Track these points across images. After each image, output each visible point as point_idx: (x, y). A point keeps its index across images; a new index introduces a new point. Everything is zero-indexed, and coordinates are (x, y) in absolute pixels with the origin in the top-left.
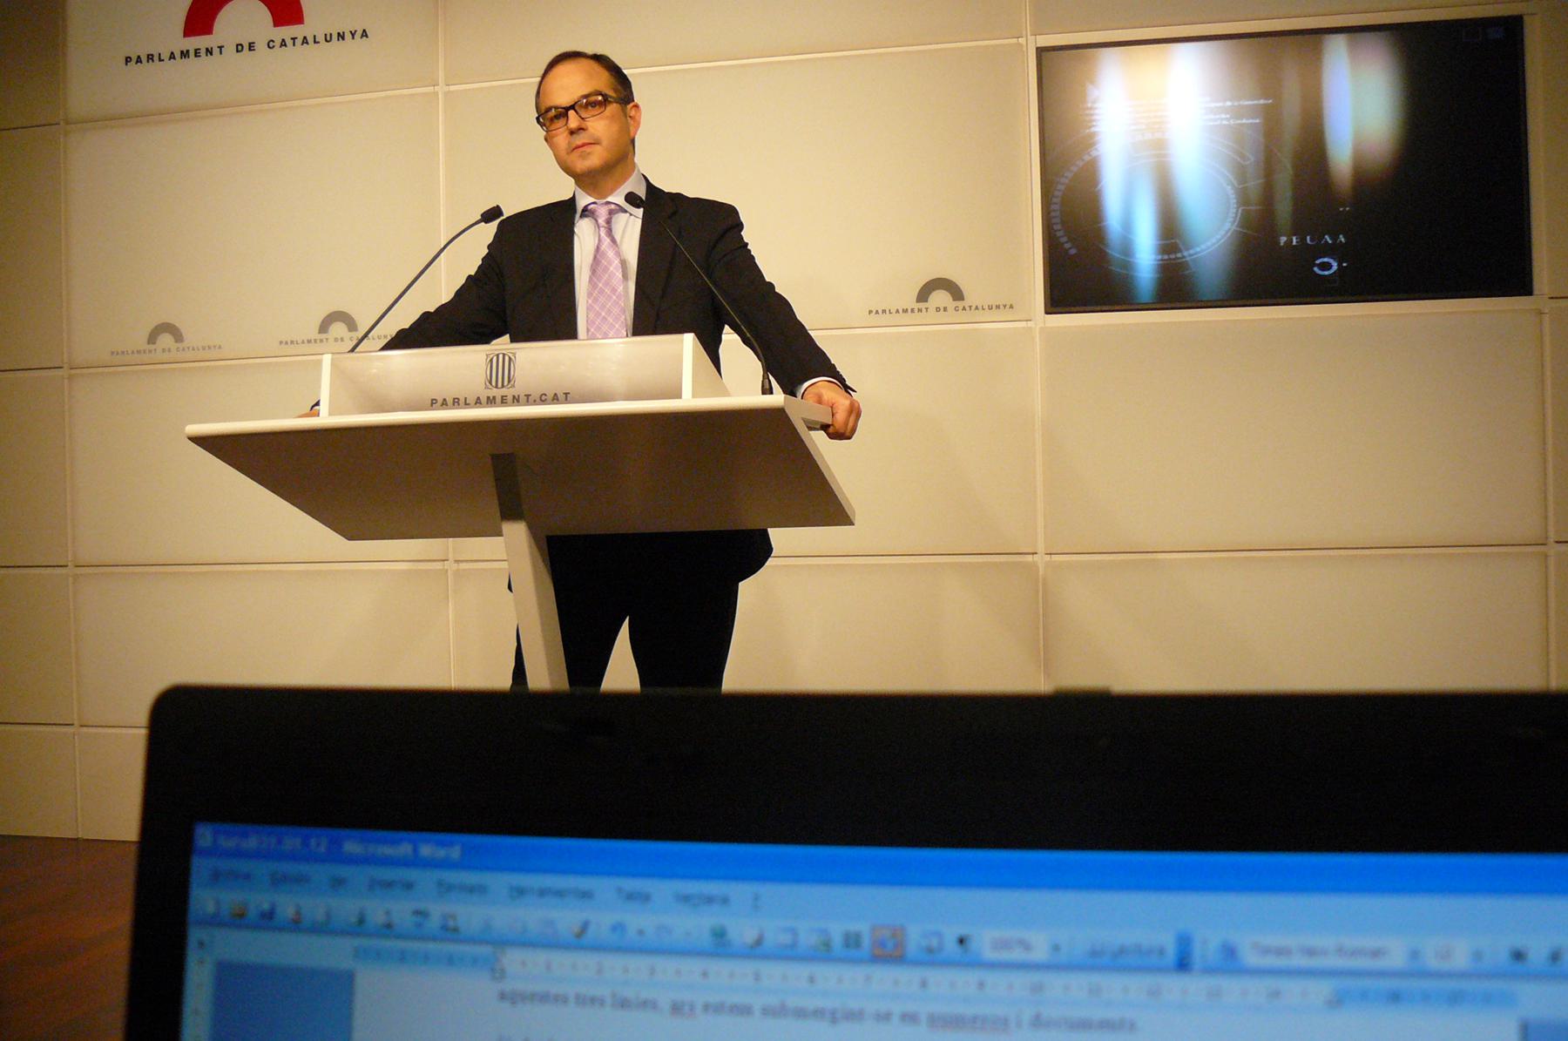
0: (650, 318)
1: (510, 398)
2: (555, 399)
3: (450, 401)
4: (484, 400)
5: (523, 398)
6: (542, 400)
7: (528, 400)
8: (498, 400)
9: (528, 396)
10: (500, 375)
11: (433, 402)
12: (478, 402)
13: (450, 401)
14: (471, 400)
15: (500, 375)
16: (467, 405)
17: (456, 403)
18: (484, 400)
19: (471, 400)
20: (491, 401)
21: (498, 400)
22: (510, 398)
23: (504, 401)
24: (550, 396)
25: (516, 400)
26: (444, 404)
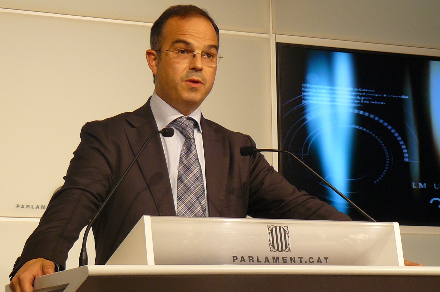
0: (219, 208)
1: (288, 259)
2: (319, 262)
3: (247, 259)
4: (271, 259)
5: (297, 260)
6: (310, 261)
7: (301, 261)
8: (281, 259)
9: (301, 258)
10: (279, 242)
11: (235, 259)
12: (267, 261)
13: (247, 259)
14: (262, 259)
15: (279, 242)
16: (259, 262)
17: (251, 260)
18: (271, 259)
19: (262, 259)
20: (276, 261)
21: (281, 259)
22: (288, 259)
23: (284, 261)
24: (316, 259)
25: (293, 261)
26: (243, 260)
